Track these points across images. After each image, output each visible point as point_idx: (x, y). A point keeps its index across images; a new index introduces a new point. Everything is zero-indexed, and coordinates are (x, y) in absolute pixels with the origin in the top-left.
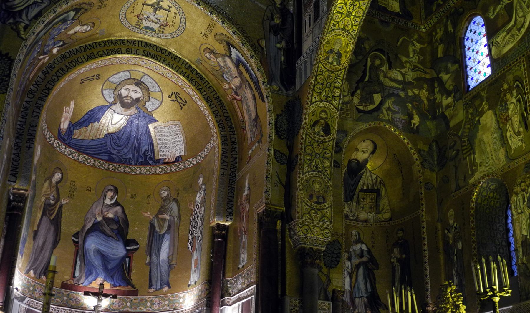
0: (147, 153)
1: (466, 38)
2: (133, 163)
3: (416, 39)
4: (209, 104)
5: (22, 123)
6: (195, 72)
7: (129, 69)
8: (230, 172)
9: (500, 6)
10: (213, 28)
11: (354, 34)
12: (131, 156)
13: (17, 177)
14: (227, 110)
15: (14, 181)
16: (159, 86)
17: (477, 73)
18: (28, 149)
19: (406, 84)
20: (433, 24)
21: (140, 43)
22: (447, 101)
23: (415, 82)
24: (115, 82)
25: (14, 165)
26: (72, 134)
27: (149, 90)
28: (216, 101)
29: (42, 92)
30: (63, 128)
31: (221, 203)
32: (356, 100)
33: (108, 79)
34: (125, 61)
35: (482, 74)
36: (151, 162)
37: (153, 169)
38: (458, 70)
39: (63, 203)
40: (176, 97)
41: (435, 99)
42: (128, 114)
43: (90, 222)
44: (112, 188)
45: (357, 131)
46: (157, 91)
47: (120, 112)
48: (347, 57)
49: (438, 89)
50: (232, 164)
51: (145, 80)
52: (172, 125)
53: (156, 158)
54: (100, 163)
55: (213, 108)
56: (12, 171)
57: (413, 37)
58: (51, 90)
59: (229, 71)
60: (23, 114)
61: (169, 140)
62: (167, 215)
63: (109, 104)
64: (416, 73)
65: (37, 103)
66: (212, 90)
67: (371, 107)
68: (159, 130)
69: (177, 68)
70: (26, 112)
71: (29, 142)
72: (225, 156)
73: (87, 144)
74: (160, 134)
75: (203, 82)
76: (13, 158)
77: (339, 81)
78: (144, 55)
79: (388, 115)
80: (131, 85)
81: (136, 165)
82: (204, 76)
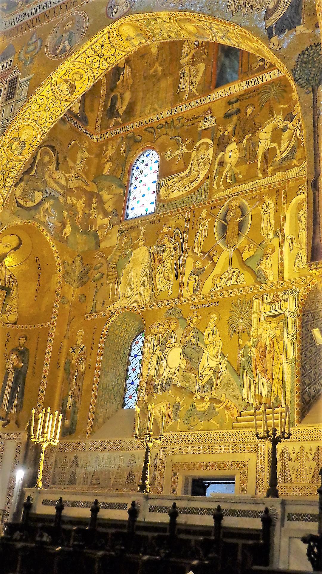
1: (136, 166)
3: (86, 147)
9: (178, 152)
11: (46, 129)
19: (68, 191)
20: (106, 139)
22: (101, 221)
32: (18, 193)
41: (90, 215)
45: (11, 225)
48: (31, 150)
49: (95, 205)
57: (83, 144)
67: (31, 204)
77: (15, 172)
79: (44, 217)
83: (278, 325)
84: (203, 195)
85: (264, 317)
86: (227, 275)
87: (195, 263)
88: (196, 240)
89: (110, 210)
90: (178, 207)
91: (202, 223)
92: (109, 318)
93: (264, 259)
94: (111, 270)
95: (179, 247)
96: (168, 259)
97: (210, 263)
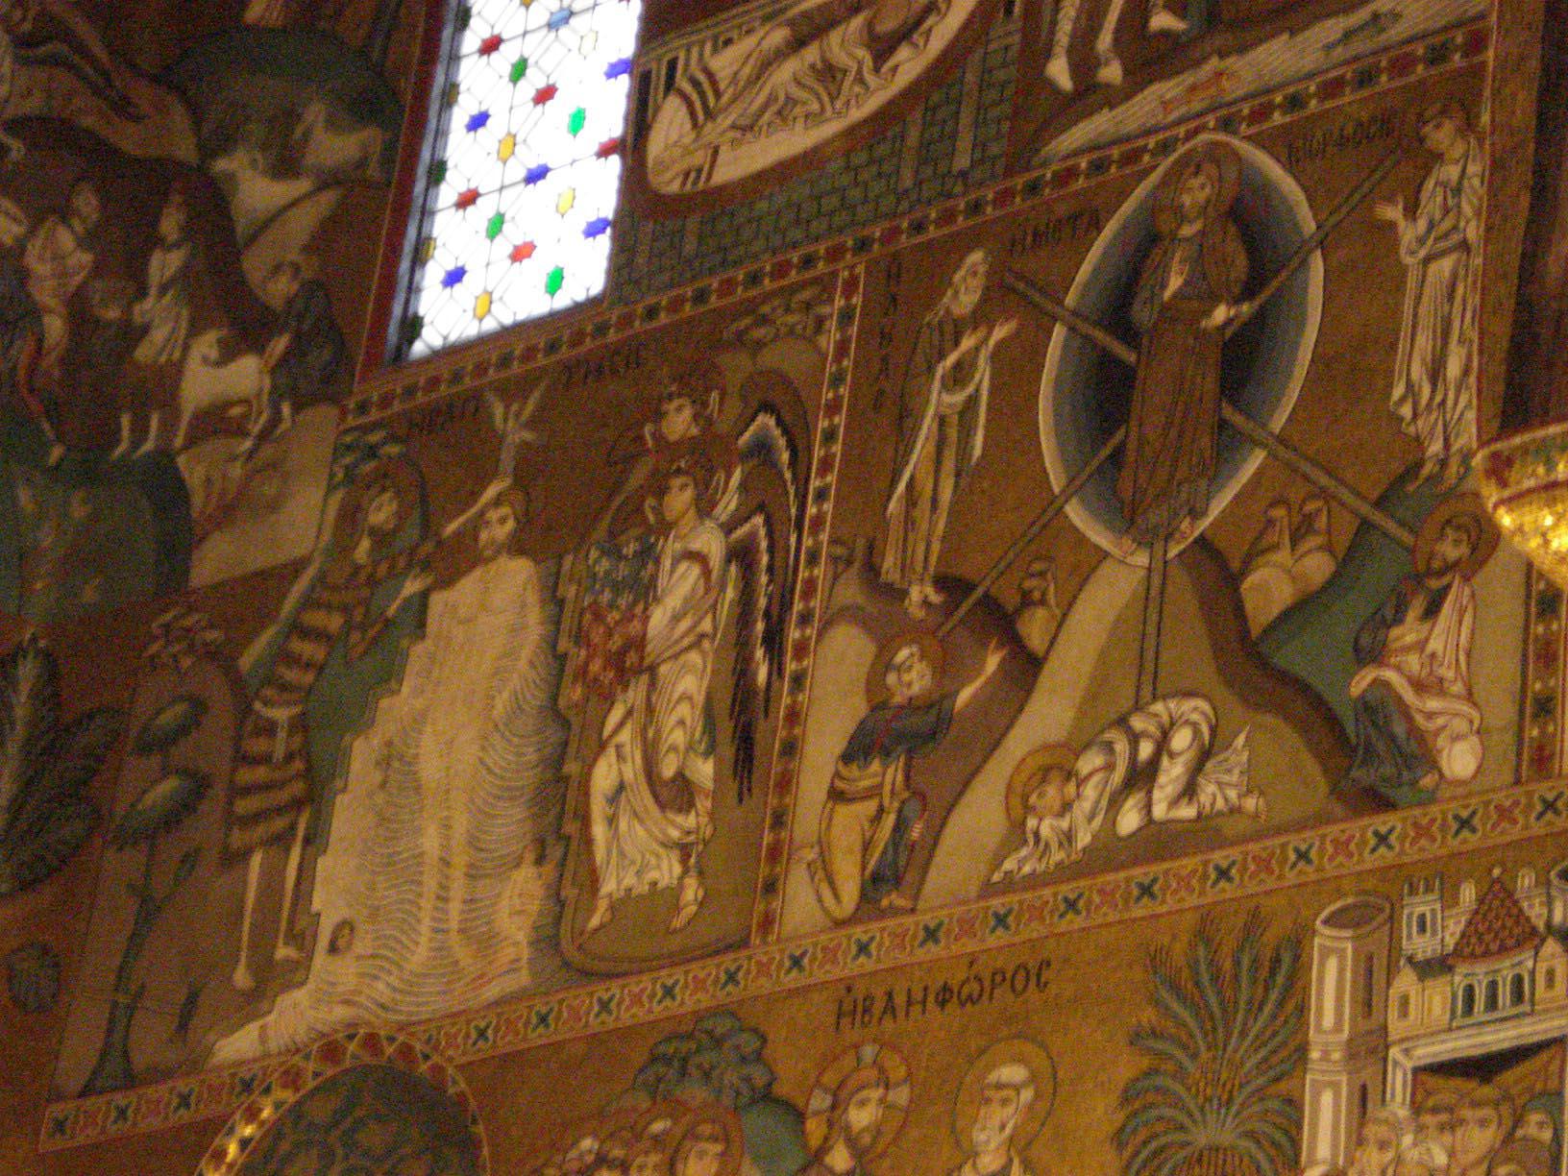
17: (504, 246)
23: (17, 149)
35: (535, 269)
38: (373, 171)
41: (133, 333)
64: (41, 74)
83: (1509, 1138)
84: (964, 142)
85: (1399, 1082)
86: (1121, 747)
87: (883, 663)
88: (901, 487)
89: (280, 289)
90: (776, 240)
91: (951, 359)
92: (220, 1125)
93: (1412, 614)
94: (258, 746)
95: (771, 549)
96: (686, 642)
97: (993, 662)
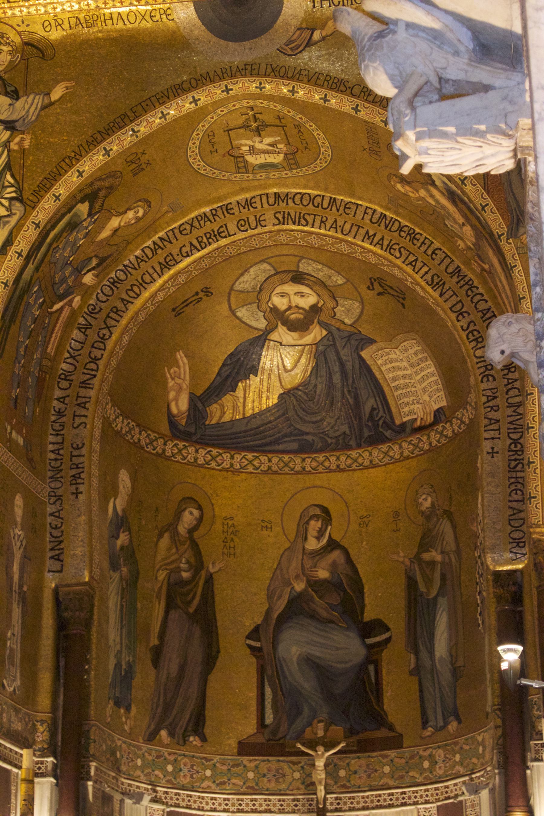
0: (378, 413)
2: (352, 443)
4: (439, 291)
5: (56, 447)
6: (396, 225)
7: (262, 258)
8: (509, 441)
10: (376, 136)
12: (345, 428)
13: (62, 561)
14: (482, 295)
15: (59, 569)
16: (339, 274)
18: (74, 496)
21: (264, 198)
24: (250, 290)
25: (53, 537)
26: (204, 418)
27: (325, 284)
28: (455, 279)
29: (85, 371)
30: (178, 413)
31: (494, 523)
33: (232, 289)
34: (244, 246)
36: (388, 434)
37: (396, 447)
39: (212, 570)
40: (381, 285)
42: (309, 342)
43: (280, 597)
44: (318, 511)
46: (340, 282)
47: (293, 342)
50: (510, 423)
51: (304, 267)
52: (405, 343)
53: (398, 422)
54: (283, 461)
55: (447, 300)
56: (52, 549)
58: (101, 361)
59: (450, 215)
60: (57, 426)
61: (410, 377)
62: (436, 551)
63: (261, 333)
65: (78, 397)
66: (440, 255)
68: (385, 358)
69: (355, 229)
70: (59, 421)
71: (74, 482)
72: (492, 407)
73: (243, 428)
74: (389, 366)
75: (419, 245)
76: (50, 524)
78: (277, 222)
80: (286, 285)
81: (359, 446)
82: (417, 230)
